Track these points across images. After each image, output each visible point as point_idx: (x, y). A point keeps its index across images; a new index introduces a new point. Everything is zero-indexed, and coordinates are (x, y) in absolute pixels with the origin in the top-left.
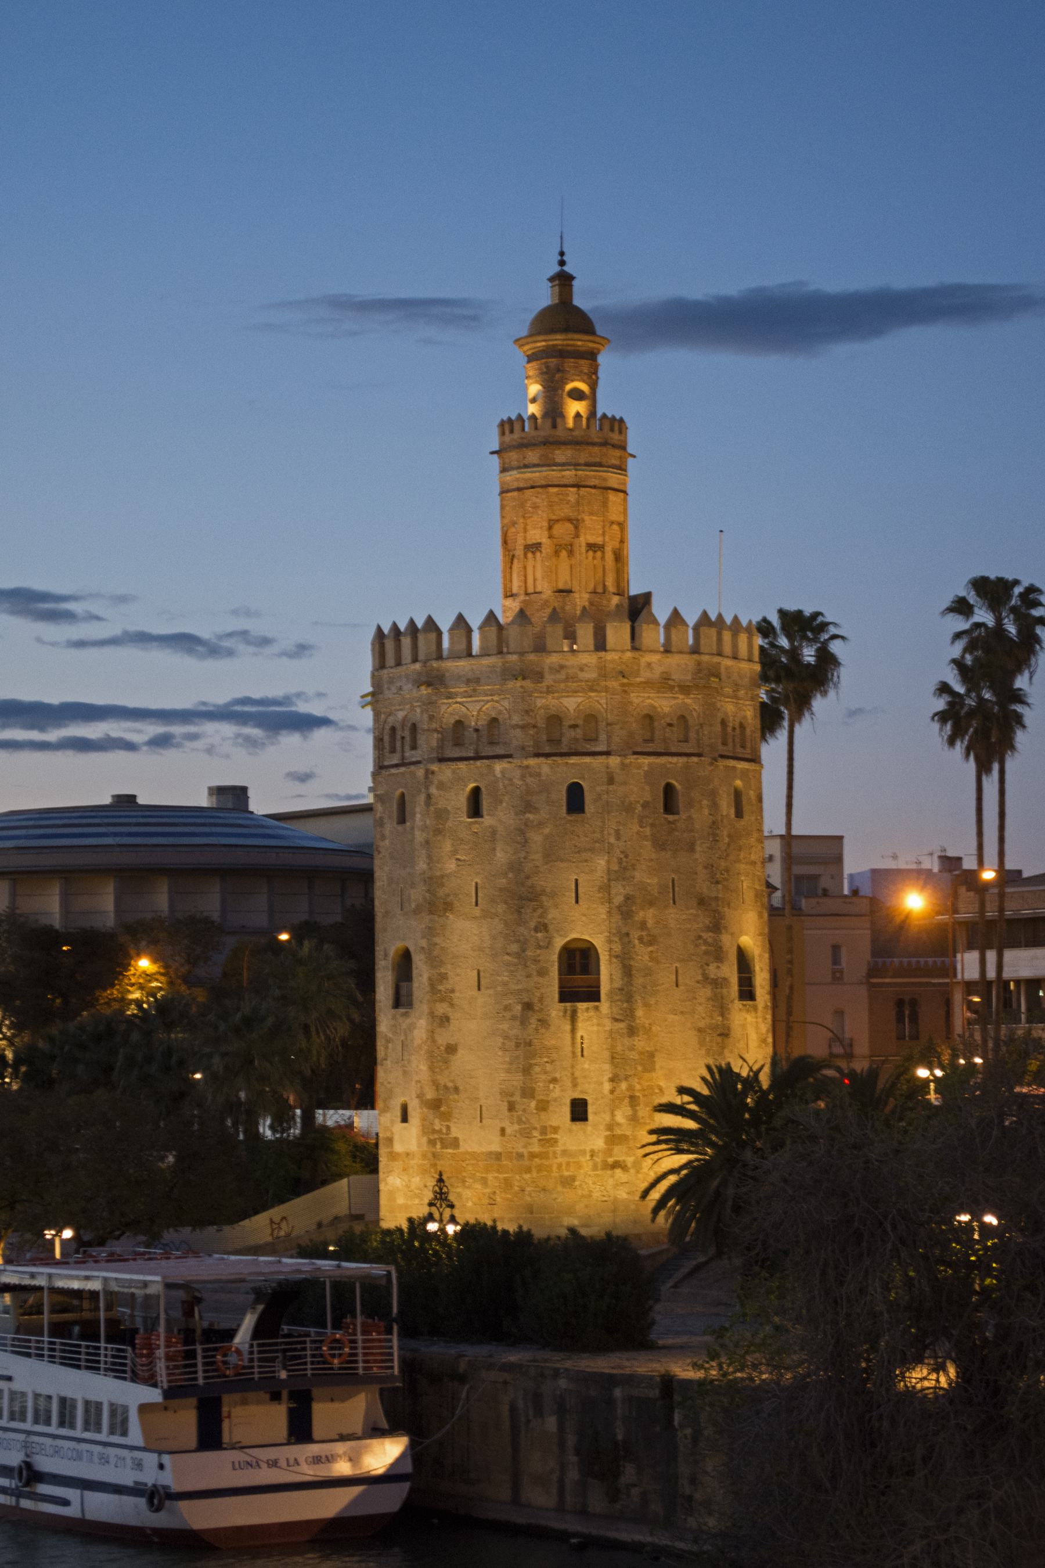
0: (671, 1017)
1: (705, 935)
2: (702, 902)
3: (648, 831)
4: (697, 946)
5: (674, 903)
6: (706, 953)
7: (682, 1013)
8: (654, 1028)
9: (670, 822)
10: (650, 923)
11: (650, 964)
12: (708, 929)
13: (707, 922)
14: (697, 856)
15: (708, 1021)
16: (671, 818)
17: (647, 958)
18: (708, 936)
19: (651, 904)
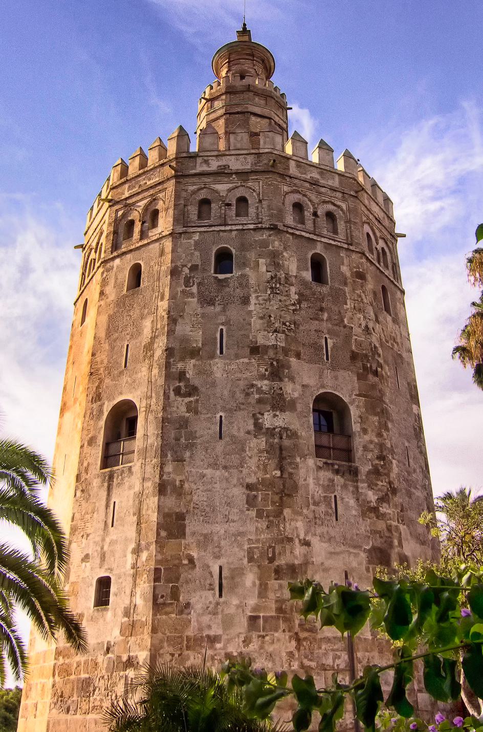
0: (209, 472)
1: (259, 383)
2: (255, 350)
3: (194, 289)
4: (248, 394)
5: (221, 352)
6: (260, 401)
7: (225, 468)
8: (186, 486)
9: (220, 280)
10: (190, 374)
11: (188, 415)
12: (262, 377)
13: (262, 370)
14: (252, 307)
15: (260, 475)
16: (221, 276)
17: (183, 409)
18: (264, 384)
19: (194, 353)
